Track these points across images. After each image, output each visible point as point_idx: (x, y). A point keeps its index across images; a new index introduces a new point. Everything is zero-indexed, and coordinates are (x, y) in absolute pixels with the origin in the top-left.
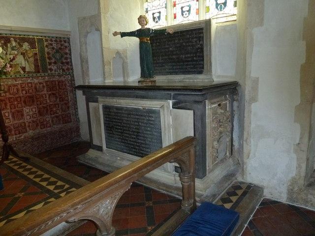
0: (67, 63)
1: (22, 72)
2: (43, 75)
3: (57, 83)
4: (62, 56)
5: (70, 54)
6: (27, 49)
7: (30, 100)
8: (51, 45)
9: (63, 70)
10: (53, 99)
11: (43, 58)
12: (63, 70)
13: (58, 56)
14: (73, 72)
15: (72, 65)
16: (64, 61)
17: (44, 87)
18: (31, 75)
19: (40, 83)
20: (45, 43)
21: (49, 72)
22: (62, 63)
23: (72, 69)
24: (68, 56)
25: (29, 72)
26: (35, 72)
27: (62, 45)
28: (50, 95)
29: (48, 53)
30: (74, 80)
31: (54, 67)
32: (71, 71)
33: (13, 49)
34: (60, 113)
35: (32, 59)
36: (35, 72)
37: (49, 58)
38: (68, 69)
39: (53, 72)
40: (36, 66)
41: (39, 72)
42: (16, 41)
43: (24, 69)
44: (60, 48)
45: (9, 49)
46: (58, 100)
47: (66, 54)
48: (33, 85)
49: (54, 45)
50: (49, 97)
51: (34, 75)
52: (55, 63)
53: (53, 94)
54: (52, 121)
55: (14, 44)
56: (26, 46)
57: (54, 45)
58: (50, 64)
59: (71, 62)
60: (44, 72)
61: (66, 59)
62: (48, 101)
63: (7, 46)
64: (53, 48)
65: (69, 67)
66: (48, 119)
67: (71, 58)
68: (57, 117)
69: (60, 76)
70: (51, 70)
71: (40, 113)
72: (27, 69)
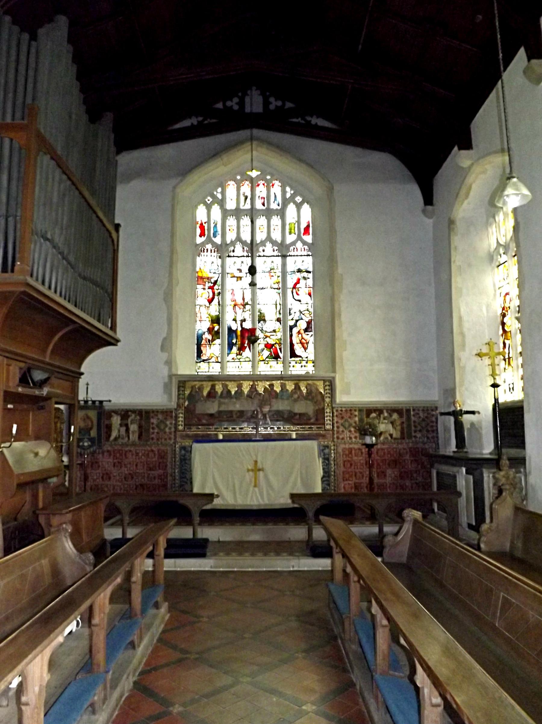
0: (433, 431)
1: (389, 438)
2: (407, 441)
3: (420, 449)
4: (428, 424)
5: (437, 423)
6: (396, 418)
7: (395, 463)
8: (418, 414)
9: (428, 438)
10: (414, 465)
11: (409, 426)
12: (428, 438)
13: (424, 424)
14: (438, 440)
15: (437, 433)
16: (430, 429)
17: (407, 453)
18: (396, 441)
19: (404, 449)
20: (412, 413)
21: (413, 439)
22: (428, 431)
23: (437, 437)
24: (434, 424)
25: (395, 439)
26: (401, 439)
27: (428, 414)
28: (412, 461)
29: (415, 422)
30: (438, 448)
31: (419, 435)
32: (436, 439)
33: (384, 419)
34: (420, 479)
35: (399, 428)
36: (401, 439)
37: (415, 427)
38: (433, 437)
39: (418, 439)
40: (402, 433)
41: (404, 438)
42: (387, 412)
43: (391, 435)
44: (426, 417)
45: (382, 419)
46: (420, 466)
47: (432, 422)
48: (398, 451)
49: (421, 414)
50: (411, 462)
51: (400, 441)
52: (420, 431)
53: (415, 460)
54: (412, 487)
55: (386, 414)
56: (395, 416)
57: (421, 414)
58: (415, 432)
59: (437, 430)
60: (408, 438)
61: (432, 426)
62: (410, 467)
63: (380, 416)
64: (420, 417)
65: (435, 434)
66: (407, 484)
67: (437, 426)
68: (416, 483)
69: (424, 443)
70: (415, 437)
71: (401, 477)
72: (394, 436)
